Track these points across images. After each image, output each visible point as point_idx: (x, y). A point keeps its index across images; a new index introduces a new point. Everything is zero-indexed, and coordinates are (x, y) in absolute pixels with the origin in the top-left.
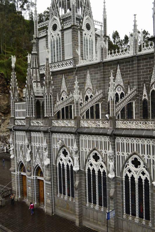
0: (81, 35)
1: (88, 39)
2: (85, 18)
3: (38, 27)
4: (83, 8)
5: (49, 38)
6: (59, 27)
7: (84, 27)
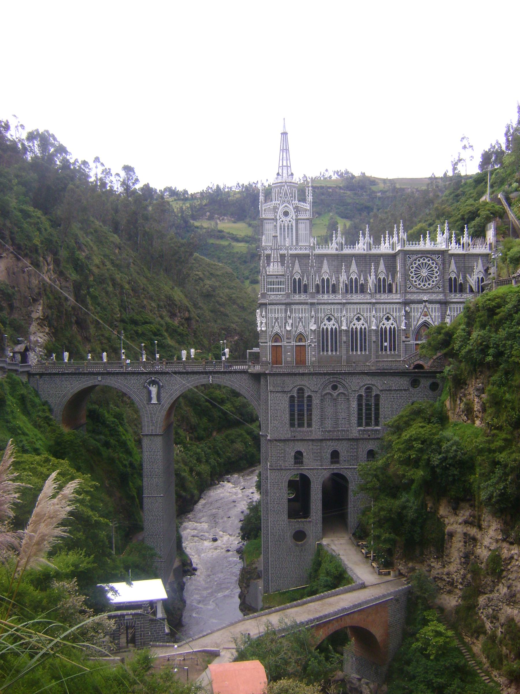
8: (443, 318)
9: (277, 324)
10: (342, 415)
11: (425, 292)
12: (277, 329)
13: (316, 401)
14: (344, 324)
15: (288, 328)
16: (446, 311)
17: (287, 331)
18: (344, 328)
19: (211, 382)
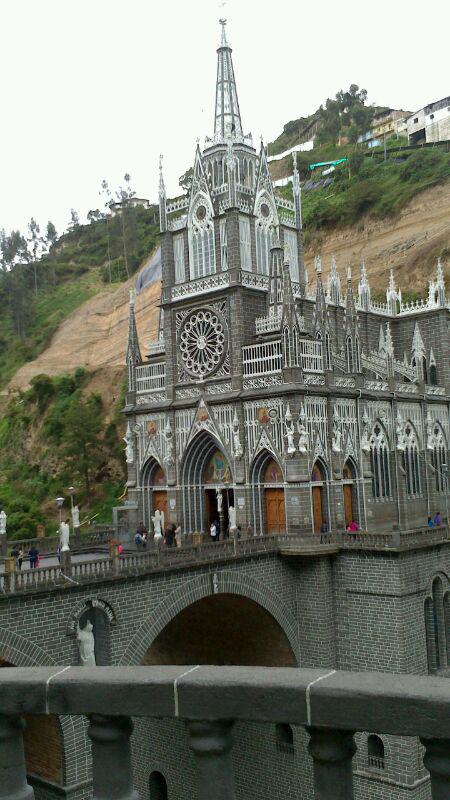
0: (252, 226)
1: (266, 233)
2: (258, 195)
3: (167, 212)
4: (255, 176)
5: (190, 233)
6: (210, 211)
7: (257, 211)
9: (318, 439)
12: (319, 451)
14: (401, 439)
15: (337, 448)
17: (335, 453)
18: (401, 447)
19: (216, 592)
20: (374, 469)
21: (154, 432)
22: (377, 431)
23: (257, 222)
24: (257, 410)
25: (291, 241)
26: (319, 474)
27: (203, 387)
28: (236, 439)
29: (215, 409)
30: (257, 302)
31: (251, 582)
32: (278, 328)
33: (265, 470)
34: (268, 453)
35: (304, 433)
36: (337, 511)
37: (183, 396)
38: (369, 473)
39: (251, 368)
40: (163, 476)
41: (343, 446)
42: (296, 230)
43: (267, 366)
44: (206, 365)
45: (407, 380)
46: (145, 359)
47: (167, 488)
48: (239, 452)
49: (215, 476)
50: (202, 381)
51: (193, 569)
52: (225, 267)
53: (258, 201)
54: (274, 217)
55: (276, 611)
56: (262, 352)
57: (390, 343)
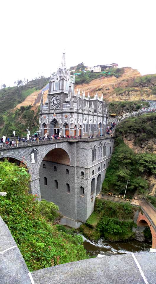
0: (66, 82)
2: (68, 77)
6: (59, 79)
7: (67, 80)
8: (103, 121)
10: (100, 154)
11: (100, 113)
12: (76, 123)
13: (97, 150)
15: (79, 123)
16: (103, 119)
19: (57, 147)
20: (85, 127)
21: (45, 118)
22: (86, 120)
23: (67, 81)
24: (65, 115)
25: (72, 85)
26: (75, 127)
27: (55, 110)
28: (61, 120)
29: (57, 114)
30: (66, 95)
31: (63, 146)
32: (70, 100)
33: (66, 126)
34: (66, 123)
35: (74, 120)
36: (78, 134)
37: (51, 112)
38: (84, 128)
39: (64, 107)
40: (46, 126)
41: (80, 123)
42: (74, 84)
43: (67, 107)
44: (56, 106)
45: (90, 111)
46: (44, 104)
47: (47, 128)
48: (61, 123)
49: (56, 127)
50: (55, 109)
51: (53, 143)
52: (61, 89)
53: (68, 78)
54: (70, 81)
55: (67, 151)
56: (66, 105)
57: (88, 105)
